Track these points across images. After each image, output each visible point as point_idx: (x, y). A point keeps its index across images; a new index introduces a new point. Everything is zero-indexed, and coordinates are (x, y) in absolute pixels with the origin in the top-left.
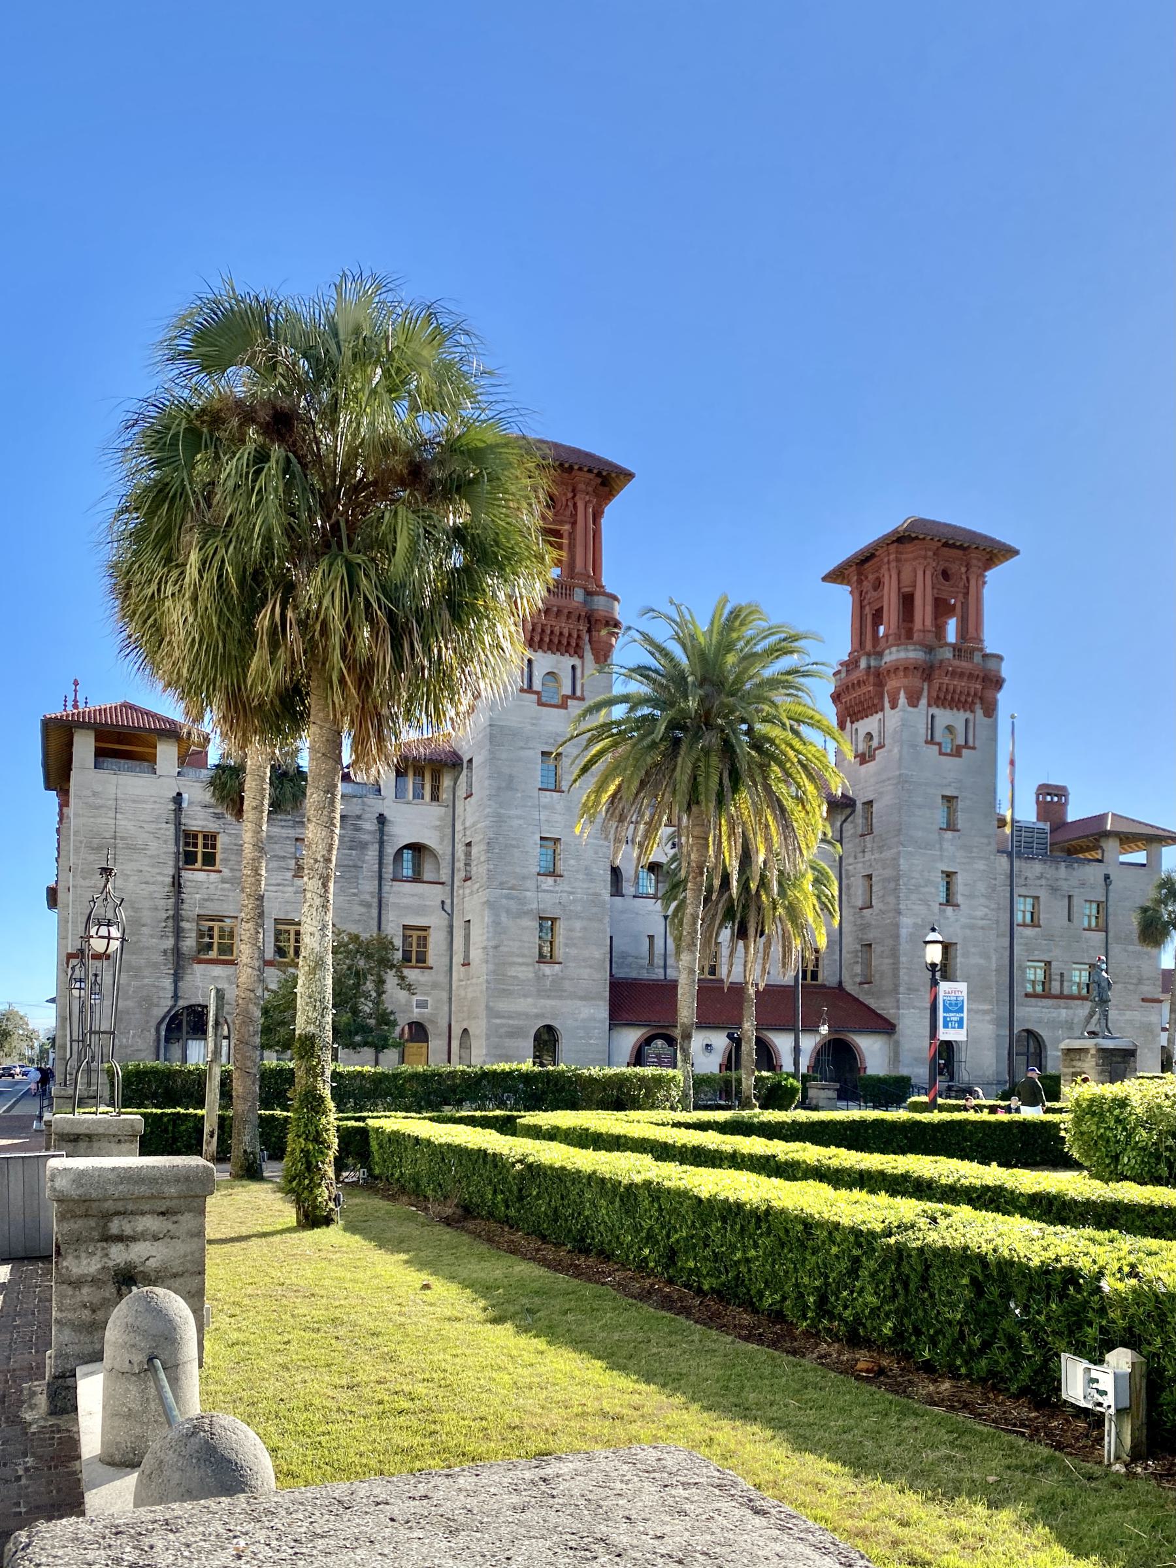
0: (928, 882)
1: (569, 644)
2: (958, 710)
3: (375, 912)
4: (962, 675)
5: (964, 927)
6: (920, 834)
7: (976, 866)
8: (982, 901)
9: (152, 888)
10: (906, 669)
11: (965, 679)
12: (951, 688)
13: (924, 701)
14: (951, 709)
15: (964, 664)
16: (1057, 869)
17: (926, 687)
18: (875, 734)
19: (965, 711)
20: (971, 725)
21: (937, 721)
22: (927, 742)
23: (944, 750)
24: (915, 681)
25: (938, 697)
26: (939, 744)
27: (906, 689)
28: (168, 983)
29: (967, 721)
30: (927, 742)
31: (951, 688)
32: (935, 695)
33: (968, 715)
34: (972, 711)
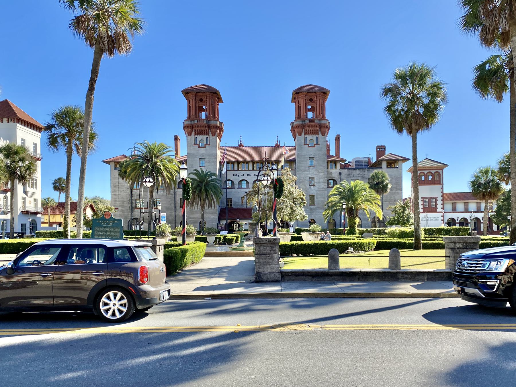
0: (306, 180)
1: (200, 133)
2: (314, 135)
3: (174, 196)
4: (312, 126)
5: (317, 191)
6: (303, 168)
7: (320, 175)
8: (323, 184)
9: (126, 194)
10: (297, 127)
12: (310, 130)
13: (303, 134)
14: (312, 135)
15: (312, 123)
16: (364, 171)
19: (316, 135)
22: (304, 144)
24: (300, 130)
25: (306, 132)
26: (308, 145)
27: (297, 131)
28: (130, 214)
29: (317, 137)
31: (310, 130)
33: (317, 136)
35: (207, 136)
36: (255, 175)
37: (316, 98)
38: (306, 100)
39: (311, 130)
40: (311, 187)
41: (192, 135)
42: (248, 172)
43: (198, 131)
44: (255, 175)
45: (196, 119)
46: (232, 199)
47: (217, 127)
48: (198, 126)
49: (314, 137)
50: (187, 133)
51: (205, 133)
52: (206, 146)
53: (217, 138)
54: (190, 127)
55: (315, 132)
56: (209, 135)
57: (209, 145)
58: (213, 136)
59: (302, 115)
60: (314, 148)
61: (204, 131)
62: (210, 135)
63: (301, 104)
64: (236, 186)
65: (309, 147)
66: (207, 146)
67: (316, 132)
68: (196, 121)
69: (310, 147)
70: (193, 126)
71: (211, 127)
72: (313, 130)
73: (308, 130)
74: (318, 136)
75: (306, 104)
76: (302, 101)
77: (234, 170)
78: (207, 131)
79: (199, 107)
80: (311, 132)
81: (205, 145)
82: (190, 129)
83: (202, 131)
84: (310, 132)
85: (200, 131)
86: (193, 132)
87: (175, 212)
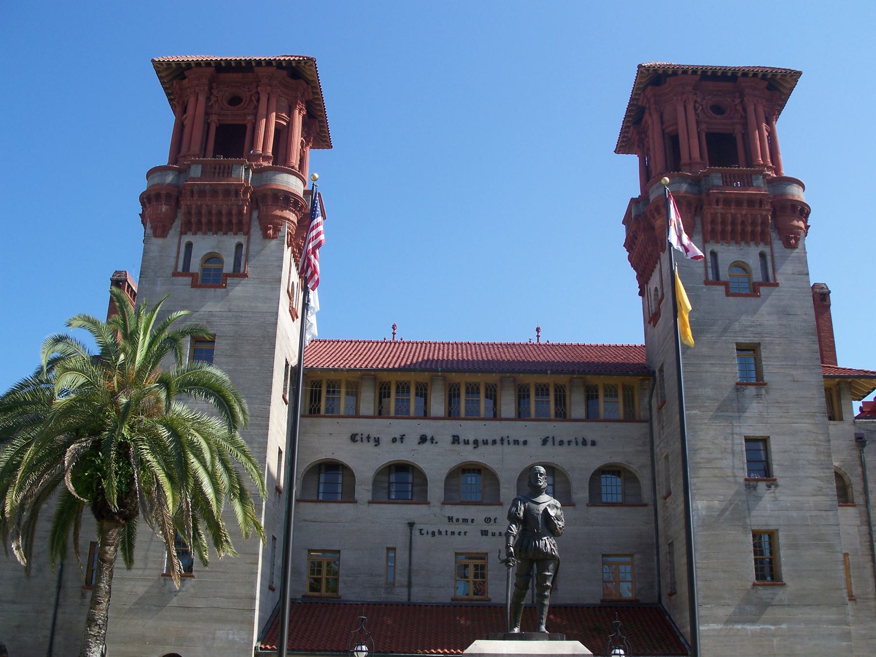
2: (747, 243)
11: (745, 206)
14: (736, 243)
17: (698, 221)
18: (659, 288)
19: (757, 244)
20: (769, 258)
21: (720, 257)
22: (707, 282)
23: (732, 291)
25: (713, 231)
26: (726, 284)
29: (762, 255)
30: (707, 282)
32: (709, 227)
33: (762, 248)
34: (768, 243)
35: (241, 239)
36: (456, 440)
37: (737, 101)
38: (696, 109)
39: (733, 223)
40: (755, 488)
41: (172, 232)
42: (426, 427)
43: (199, 213)
44: (456, 440)
45: (197, 163)
46: (339, 551)
47: (287, 199)
48: (202, 193)
49: (751, 255)
50: (149, 225)
51: (230, 222)
52: (229, 280)
53: (287, 253)
54: (168, 196)
55: (753, 233)
56: (248, 234)
57: (245, 275)
58: (266, 236)
59: (685, 158)
60: (753, 299)
61: (230, 213)
62: (256, 231)
63: (677, 124)
64: (363, 492)
65: (728, 294)
66: (236, 280)
67: (759, 229)
68: (196, 171)
69: (733, 295)
70: (180, 193)
71: (264, 197)
72: (743, 223)
73: (723, 223)
74: (767, 250)
75: (698, 123)
76: (681, 109)
77: (357, 416)
78: (240, 212)
79: (223, 129)
80: (733, 231)
81: (228, 275)
82: (164, 208)
83: (220, 213)
84: (729, 228)
85: (210, 213)
86: (178, 223)
87: (57, 605)
